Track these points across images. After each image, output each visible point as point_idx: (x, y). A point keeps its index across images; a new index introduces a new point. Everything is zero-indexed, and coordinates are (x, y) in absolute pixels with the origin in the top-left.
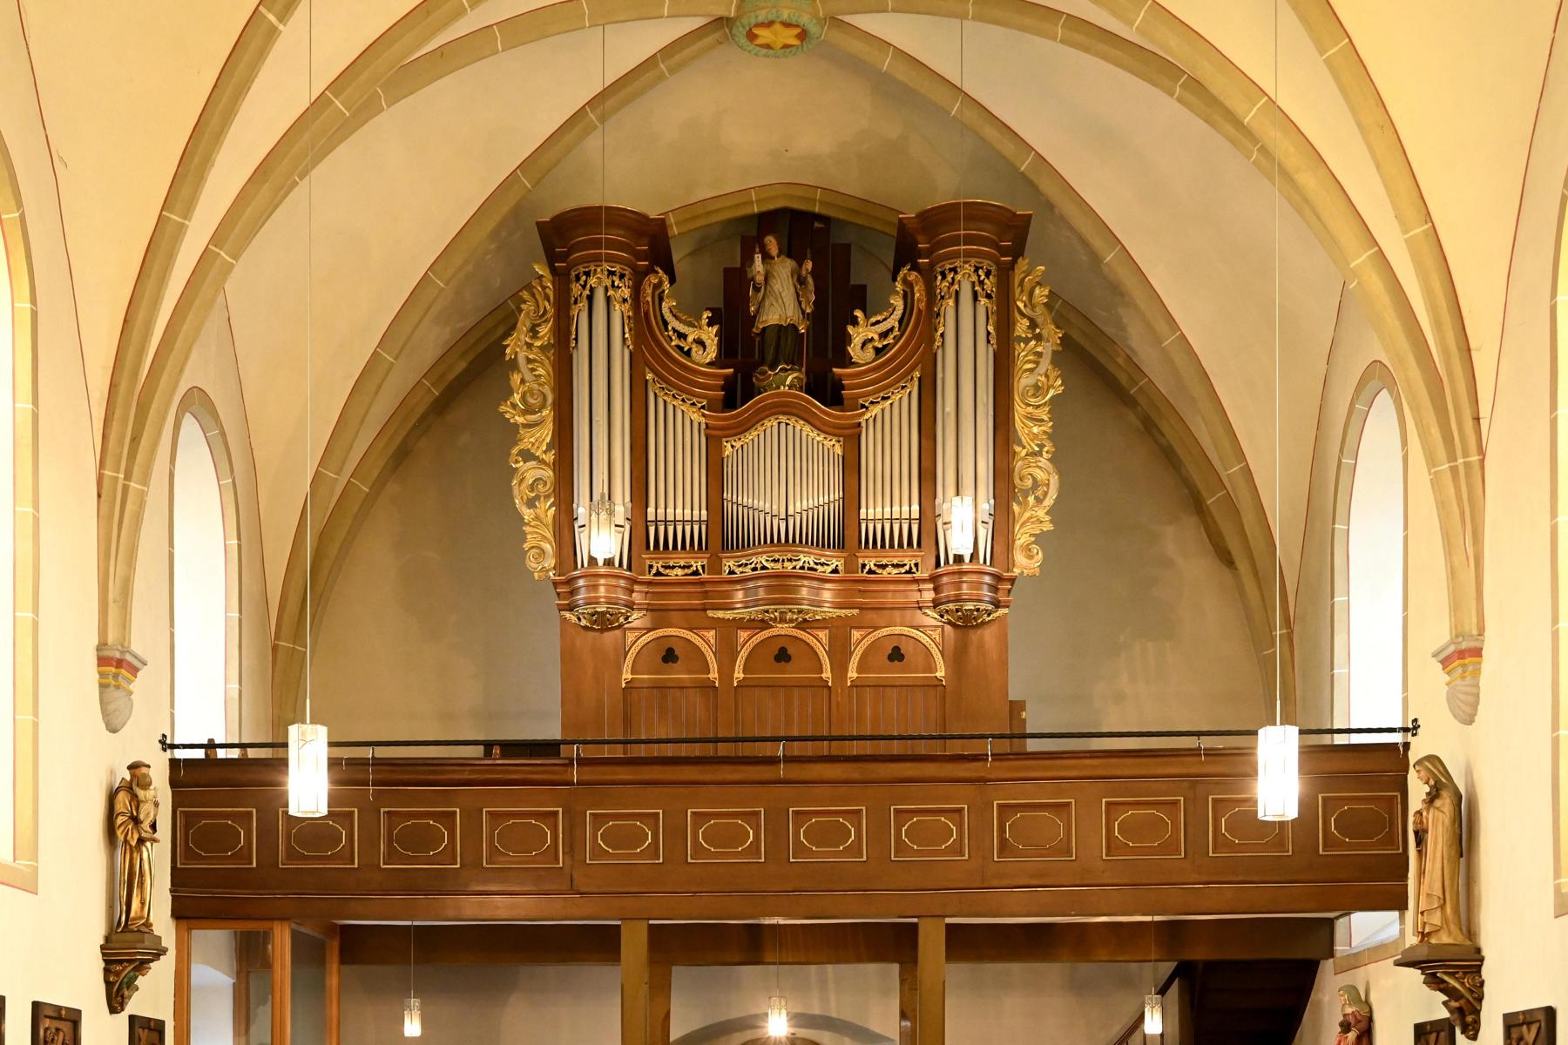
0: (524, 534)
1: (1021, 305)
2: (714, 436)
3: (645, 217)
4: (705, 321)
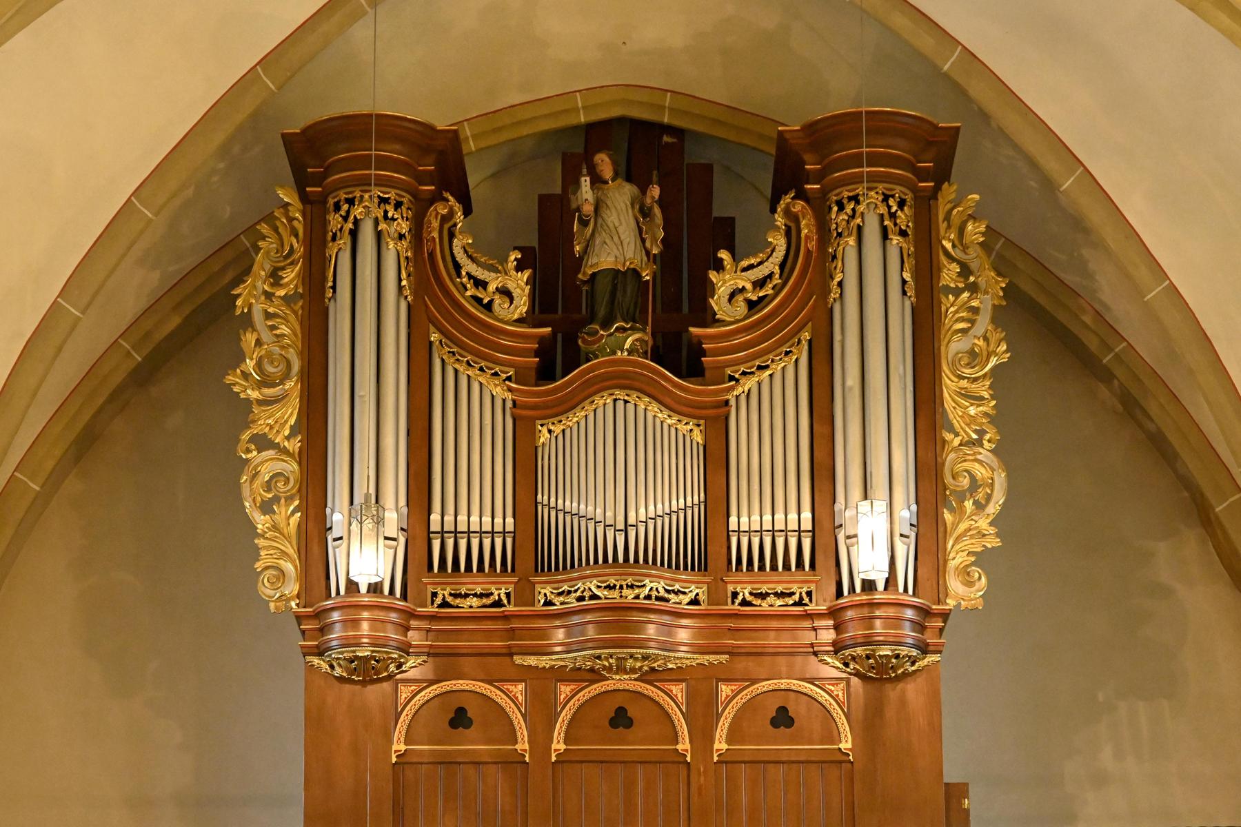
0: (257, 549)
1: (948, 245)
2: (523, 418)
3: (431, 128)
4: (512, 264)
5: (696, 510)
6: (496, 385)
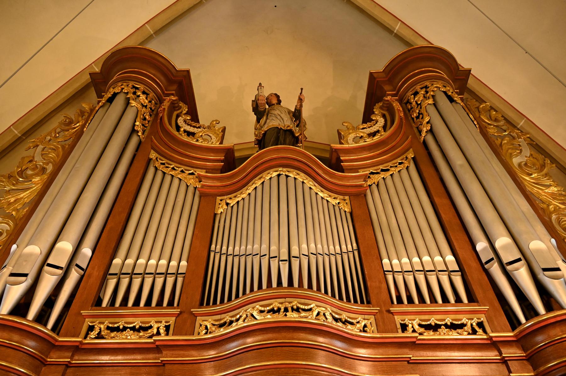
5: (351, 255)
6: (190, 179)
